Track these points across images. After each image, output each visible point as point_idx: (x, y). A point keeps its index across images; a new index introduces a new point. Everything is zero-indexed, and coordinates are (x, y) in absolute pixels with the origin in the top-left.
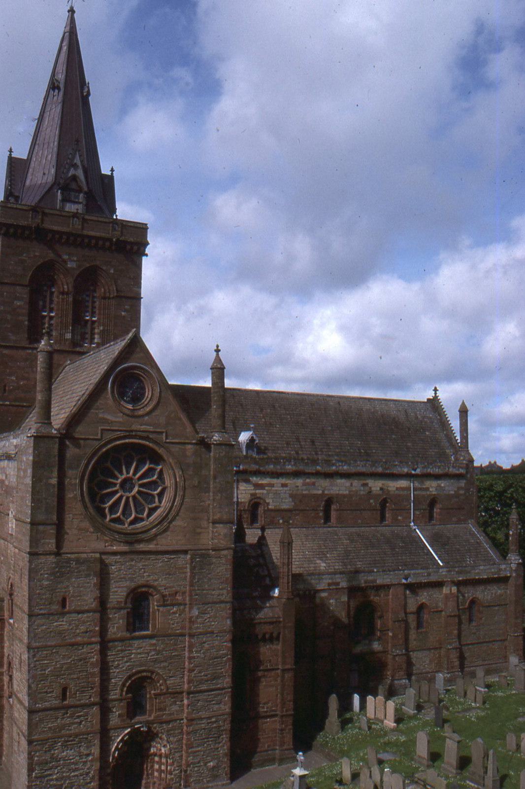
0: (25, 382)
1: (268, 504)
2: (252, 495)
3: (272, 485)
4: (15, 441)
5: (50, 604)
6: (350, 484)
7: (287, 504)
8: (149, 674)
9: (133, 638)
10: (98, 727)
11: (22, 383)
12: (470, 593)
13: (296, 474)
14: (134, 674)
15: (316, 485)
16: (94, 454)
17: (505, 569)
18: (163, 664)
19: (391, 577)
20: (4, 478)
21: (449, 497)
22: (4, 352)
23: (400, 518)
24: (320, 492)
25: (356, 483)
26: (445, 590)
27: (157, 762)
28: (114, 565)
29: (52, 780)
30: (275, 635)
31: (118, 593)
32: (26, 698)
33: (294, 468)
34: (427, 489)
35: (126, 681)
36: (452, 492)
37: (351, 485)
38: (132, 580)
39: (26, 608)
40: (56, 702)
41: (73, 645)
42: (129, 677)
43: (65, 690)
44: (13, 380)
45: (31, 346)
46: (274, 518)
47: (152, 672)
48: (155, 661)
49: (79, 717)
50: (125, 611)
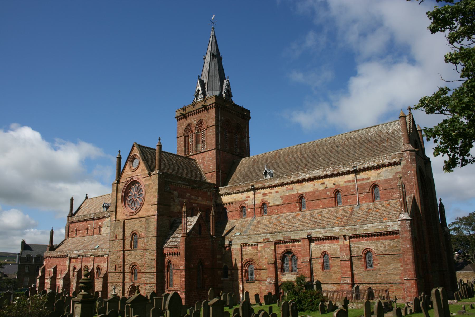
1: (269, 203)
2: (262, 200)
6: (313, 185)
8: (136, 264)
10: (122, 281)
12: (364, 244)
13: (282, 185)
15: (294, 189)
19: (299, 234)
23: (348, 201)
24: (296, 192)
25: (317, 183)
26: (341, 241)
30: (179, 253)
31: (128, 234)
37: (314, 185)
43: (116, 266)
46: (273, 210)
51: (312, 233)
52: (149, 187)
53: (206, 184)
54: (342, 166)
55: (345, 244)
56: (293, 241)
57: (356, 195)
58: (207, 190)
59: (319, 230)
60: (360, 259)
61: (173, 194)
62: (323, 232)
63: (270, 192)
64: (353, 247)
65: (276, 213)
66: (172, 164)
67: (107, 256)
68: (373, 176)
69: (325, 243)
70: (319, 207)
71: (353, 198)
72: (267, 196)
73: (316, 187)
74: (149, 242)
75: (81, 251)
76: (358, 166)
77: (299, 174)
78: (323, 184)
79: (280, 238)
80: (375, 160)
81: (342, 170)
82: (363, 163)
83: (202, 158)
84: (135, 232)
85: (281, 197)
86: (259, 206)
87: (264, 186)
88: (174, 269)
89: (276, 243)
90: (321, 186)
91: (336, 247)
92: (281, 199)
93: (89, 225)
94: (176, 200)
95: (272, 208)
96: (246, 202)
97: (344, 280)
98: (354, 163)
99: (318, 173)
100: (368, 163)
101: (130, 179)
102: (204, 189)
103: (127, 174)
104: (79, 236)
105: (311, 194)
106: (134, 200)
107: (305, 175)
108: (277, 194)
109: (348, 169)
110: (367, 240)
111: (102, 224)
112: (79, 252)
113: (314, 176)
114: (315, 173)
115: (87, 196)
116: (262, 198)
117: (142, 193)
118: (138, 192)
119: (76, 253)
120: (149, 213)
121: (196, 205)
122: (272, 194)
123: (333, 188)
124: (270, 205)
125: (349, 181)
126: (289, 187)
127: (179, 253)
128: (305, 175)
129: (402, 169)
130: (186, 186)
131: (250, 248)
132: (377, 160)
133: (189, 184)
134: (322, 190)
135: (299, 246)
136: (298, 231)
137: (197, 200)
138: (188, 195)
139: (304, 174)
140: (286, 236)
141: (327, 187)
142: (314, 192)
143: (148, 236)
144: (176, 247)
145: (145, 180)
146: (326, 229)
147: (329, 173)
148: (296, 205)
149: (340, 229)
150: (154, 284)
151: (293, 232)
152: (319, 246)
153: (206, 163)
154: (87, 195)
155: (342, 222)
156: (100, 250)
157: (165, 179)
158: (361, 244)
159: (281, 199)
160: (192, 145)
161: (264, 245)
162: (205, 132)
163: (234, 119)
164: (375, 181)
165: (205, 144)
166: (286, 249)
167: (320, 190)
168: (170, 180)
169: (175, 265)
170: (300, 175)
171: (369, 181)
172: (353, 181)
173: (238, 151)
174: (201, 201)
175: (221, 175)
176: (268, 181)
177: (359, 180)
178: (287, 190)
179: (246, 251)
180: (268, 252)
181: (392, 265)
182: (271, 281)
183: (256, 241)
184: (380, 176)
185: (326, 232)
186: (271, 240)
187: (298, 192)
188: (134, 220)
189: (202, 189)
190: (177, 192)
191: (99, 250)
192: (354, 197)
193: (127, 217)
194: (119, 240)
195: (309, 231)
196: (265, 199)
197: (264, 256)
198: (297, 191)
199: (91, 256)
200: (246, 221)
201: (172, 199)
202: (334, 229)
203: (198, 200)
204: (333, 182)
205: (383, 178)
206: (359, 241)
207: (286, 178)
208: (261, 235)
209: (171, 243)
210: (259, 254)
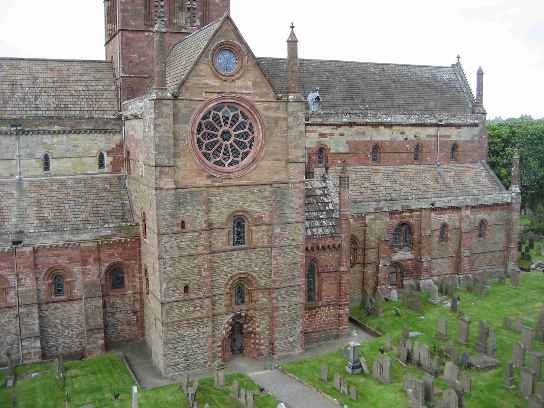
0: (145, 58)
2: (318, 142)
3: (332, 134)
4: (140, 105)
5: (173, 225)
7: (344, 149)
9: (234, 250)
11: (142, 59)
12: (481, 215)
13: (351, 125)
14: (234, 276)
16: (200, 112)
17: (507, 197)
18: (255, 269)
20: (134, 133)
21: (466, 142)
22: (128, 35)
23: (428, 159)
24: (369, 139)
27: (254, 338)
28: (218, 196)
29: (180, 350)
30: (337, 246)
32: (159, 294)
33: (350, 120)
34: (450, 136)
35: (229, 280)
36: (469, 139)
37: (392, 133)
38: (231, 206)
39: (155, 229)
40: (180, 297)
41: (191, 255)
42: (231, 278)
44: (136, 58)
45: (148, 30)
46: (334, 159)
47: (248, 275)
48: (249, 267)
49: (197, 307)
50: (227, 230)
51: (435, 201)
52: (276, 123)
54: (429, 116)
57: (436, 153)
59: (444, 199)
60: (475, 230)
62: (447, 201)
63: (331, 133)
65: (338, 164)
68: (454, 134)
69: (445, 213)
70: (396, 162)
71: (433, 156)
72: (327, 137)
73: (394, 136)
74: (287, 233)
76: (445, 120)
77: (378, 115)
78: (403, 133)
79: (397, 207)
81: (428, 121)
82: (449, 118)
85: (347, 142)
86: (315, 152)
87: (325, 122)
88: (323, 272)
89: (392, 213)
90: (401, 136)
92: (347, 145)
95: (334, 156)
97: (464, 253)
98: (441, 116)
100: (453, 119)
101: (216, 96)
103: (204, 81)
105: (388, 144)
106: (226, 146)
107: (385, 118)
108: (343, 137)
109: (434, 122)
110: (483, 210)
113: (396, 121)
114: (398, 119)
116: (317, 140)
118: (234, 127)
120: (278, 177)
122: (335, 137)
123: (414, 141)
124: (331, 151)
125: (431, 136)
126: (360, 130)
127: (337, 246)
128: (385, 118)
129: (479, 132)
132: (462, 118)
134: (402, 141)
135: (420, 216)
136: (421, 199)
139: (384, 117)
140: (405, 204)
141: (407, 139)
142: (391, 142)
143: (284, 221)
144: (332, 236)
145: (266, 109)
146: (451, 198)
147: (414, 121)
148: (367, 156)
149: (464, 199)
150: (301, 305)
151: (413, 200)
152: (438, 216)
159: (347, 145)
160: (159, 7)
161: (375, 217)
164: (456, 141)
167: (399, 141)
169: (326, 266)
170: (379, 117)
171: (449, 139)
172: (436, 136)
176: (333, 116)
177: (441, 136)
178: (356, 134)
180: (380, 225)
181: (499, 234)
182: (386, 263)
183: (364, 211)
184: (460, 136)
186: (385, 209)
187: (371, 139)
188: (238, 188)
192: (434, 155)
193: (213, 182)
194: (194, 232)
195: (433, 200)
196: (324, 141)
197: (375, 231)
198: (370, 136)
202: (459, 198)
204: (415, 134)
205: (462, 139)
206: (477, 211)
207: (359, 116)
208: (371, 203)
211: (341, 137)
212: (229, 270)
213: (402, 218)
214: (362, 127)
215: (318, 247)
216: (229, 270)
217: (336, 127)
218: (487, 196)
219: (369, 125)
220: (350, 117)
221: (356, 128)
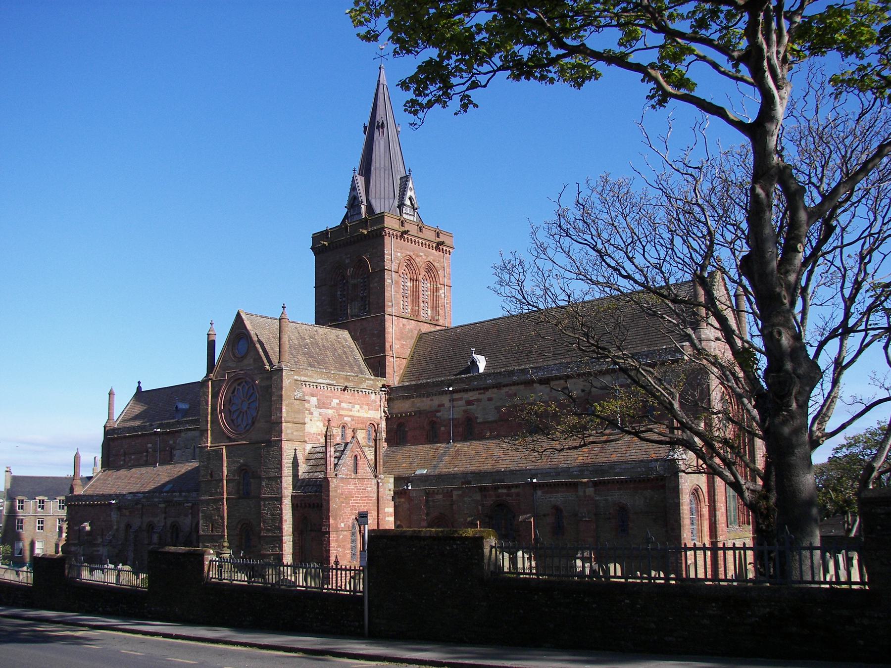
3: (479, 400)
12: (617, 496)
53: (367, 381)
55: (587, 494)
56: (509, 487)
58: (370, 391)
61: (308, 402)
63: (479, 399)
64: (598, 500)
66: (306, 345)
67: (190, 504)
69: (557, 492)
72: (474, 405)
75: (140, 495)
80: (648, 354)
83: (361, 330)
84: (244, 468)
89: (482, 489)
91: (573, 498)
93: (150, 445)
94: (314, 413)
96: (438, 414)
99: (557, 369)
102: (364, 390)
103: (227, 365)
104: (130, 465)
110: (619, 489)
111: (175, 443)
112: (136, 496)
115: (141, 385)
117: (253, 393)
119: (129, 498)
121: (349, 419)
124: (479, 421)
126: (510, 392)
130: (332, 387)
131: (440, 497)
133: (336, 383)
135: (518, 495)
137: (351, 411)
138: (336, 401)
152: (548, 496)
153: (367, 339)
154: (139, 383)
155: (589, 457)
156: (177, 494)
157: (296, 377)
158: (612, 495)
162: (366, 280)
163: (421, 254)
165: (367, 302)
166: (498, 499)
168: (303, 378)
173: (429, 314)
174: (359, 411)
175: (396, 361)
176: (476, 379)
179: (433, 501)
185: (559, 475)
189: (360, 390)
190: (316, 398)
191: (174, 494)
199: (159, 503)
200: (437, 449)
201: (307, 412)
203: (353, 409)
204: (582, 387)
209: (307, 488)
210: (455, 507)
211: (488, 402)
212: (237, 515)
213: (499, 497)
214: (513, 388)
215: (305, 504)
216: (237, 515)
217: (482, 391)
218: (619, 466)
219: (518, 384)
220: (494, 377)
221: (505, 389)
